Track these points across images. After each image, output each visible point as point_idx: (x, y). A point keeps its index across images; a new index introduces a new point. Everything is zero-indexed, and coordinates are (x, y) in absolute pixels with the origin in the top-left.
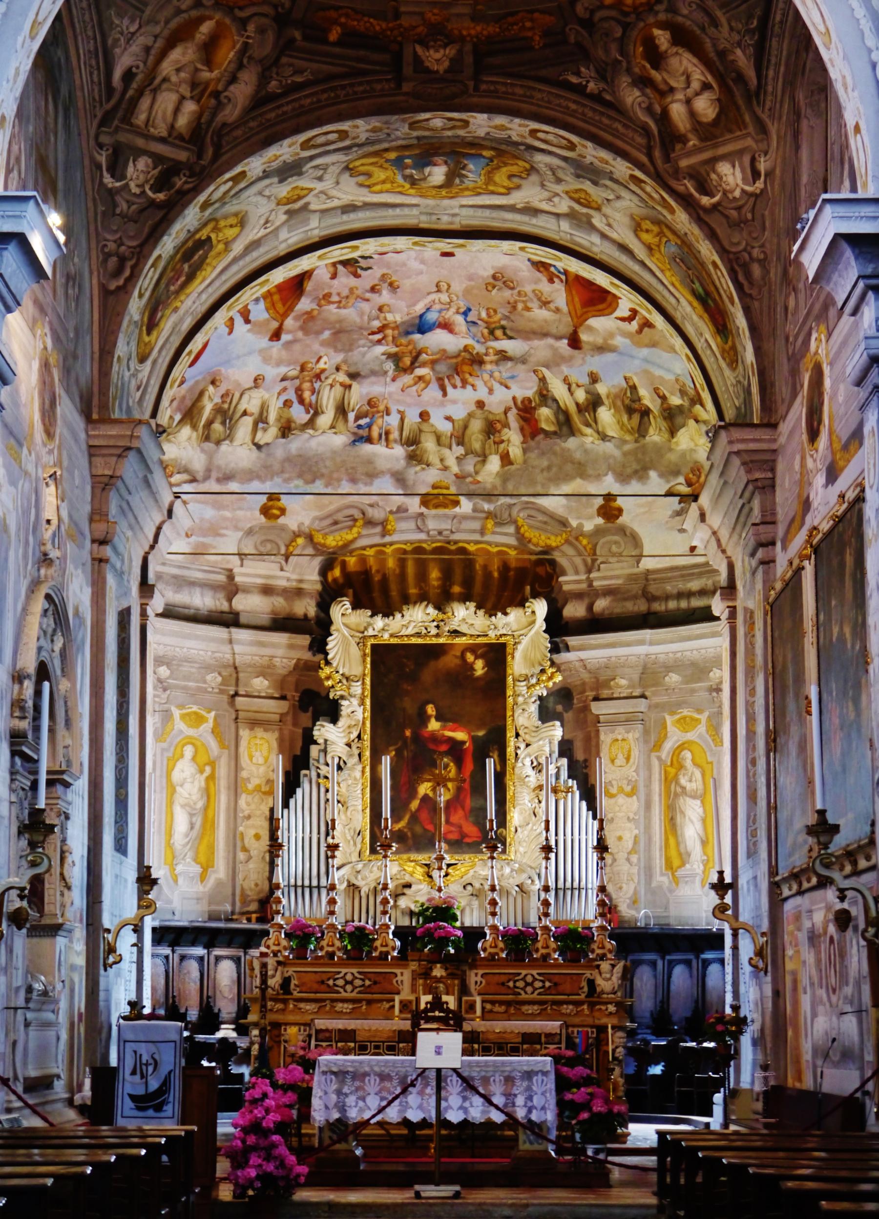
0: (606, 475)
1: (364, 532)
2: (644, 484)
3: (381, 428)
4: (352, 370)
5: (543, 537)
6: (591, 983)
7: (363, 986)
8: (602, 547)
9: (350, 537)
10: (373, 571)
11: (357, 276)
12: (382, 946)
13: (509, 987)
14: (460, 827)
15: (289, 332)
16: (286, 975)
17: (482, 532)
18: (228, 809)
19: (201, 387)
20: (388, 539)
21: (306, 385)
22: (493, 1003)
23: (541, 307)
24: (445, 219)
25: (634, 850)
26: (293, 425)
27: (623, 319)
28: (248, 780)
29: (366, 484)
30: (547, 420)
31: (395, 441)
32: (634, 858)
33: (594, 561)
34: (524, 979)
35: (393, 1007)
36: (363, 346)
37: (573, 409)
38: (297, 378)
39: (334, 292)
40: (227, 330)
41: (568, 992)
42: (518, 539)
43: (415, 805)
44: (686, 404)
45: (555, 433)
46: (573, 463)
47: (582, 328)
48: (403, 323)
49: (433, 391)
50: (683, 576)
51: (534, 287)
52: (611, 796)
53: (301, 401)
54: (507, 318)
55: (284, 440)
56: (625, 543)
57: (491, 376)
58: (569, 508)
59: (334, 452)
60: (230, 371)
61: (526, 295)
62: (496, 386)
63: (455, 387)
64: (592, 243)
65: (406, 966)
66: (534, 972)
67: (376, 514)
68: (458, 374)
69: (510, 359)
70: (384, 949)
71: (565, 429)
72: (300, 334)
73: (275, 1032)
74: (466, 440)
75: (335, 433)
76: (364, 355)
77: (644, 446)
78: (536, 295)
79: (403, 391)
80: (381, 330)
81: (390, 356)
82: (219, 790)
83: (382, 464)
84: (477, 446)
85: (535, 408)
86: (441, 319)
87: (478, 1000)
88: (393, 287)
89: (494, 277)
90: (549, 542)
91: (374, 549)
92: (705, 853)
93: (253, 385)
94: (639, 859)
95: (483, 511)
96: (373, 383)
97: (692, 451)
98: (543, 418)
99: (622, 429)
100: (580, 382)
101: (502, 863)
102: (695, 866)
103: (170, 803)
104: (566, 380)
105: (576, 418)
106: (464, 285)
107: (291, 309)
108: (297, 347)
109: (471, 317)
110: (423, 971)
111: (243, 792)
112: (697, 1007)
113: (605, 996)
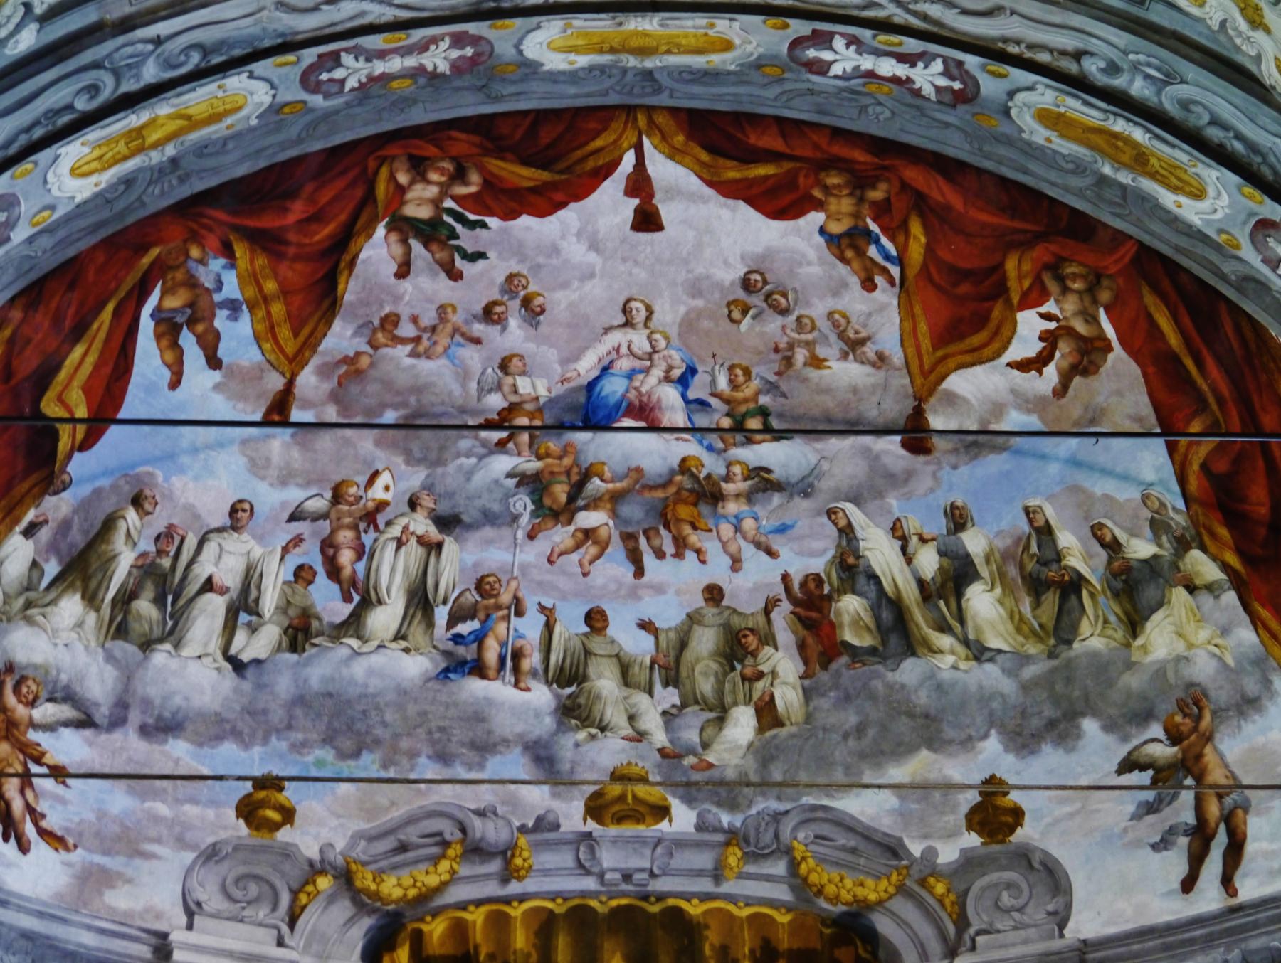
0: (985, 736)
1: (464, 871)
2: (1070, 750)
3: (503, 644)
4: (444, 508)
5: (848, 883)
8: (978, 899)
9: (433, 881)
10: (482, 958)
11: (455, 275)
15: (307, 405)
17: (717, 875)
19: (108, 507)
20: (514, 888)
21: (345, 536)
23: (844, 356)
27: (1023, 366)
29: (470, 767)
30: (857, 622)
31: (534, 674)
33: (962, 922)
37: (910, 594)
38: (325, 516)
39: (405, 312)
40: (167, 374)
42: (793, 888)
44: (1166, 552)
45: (873, 651)
46: (911, 715)
47: (933, 400)
48: (551, 401)
49: (614, 568)
50: (1167, 948)
51: (830, 304)
53: (334, 572)
54: (771, 387)
55: (294, 657)
56: (1031, 887)
57: (738, 529)
58: (901, 814)
59: (403, 692)
60: (177, 482)
61: (813, 328)
62: (748, 552)
63: (660, 555)
67: (490, 832)
69: (777, 486)
71: (894, 640)
74: (684, 672)
76: (469, 475)
77: (1069, 664)
78: (836, 325)
79: (550, 561)
83: (505, 725)
84: (706, 686)
85: (829, 598)
86: (632, 395)
88: (532, 310)
89: (746, 284)
90: (860, 892)
91: (484, 909)
93: (226, 521)
95: (718, 829)
96: (489, 542)
97: (1179, 659)
98: (846, 619)
99: (1018, 630)
104: (897, 531)
105: (919, 617)
106: (682, 310)
107: (309, 345)
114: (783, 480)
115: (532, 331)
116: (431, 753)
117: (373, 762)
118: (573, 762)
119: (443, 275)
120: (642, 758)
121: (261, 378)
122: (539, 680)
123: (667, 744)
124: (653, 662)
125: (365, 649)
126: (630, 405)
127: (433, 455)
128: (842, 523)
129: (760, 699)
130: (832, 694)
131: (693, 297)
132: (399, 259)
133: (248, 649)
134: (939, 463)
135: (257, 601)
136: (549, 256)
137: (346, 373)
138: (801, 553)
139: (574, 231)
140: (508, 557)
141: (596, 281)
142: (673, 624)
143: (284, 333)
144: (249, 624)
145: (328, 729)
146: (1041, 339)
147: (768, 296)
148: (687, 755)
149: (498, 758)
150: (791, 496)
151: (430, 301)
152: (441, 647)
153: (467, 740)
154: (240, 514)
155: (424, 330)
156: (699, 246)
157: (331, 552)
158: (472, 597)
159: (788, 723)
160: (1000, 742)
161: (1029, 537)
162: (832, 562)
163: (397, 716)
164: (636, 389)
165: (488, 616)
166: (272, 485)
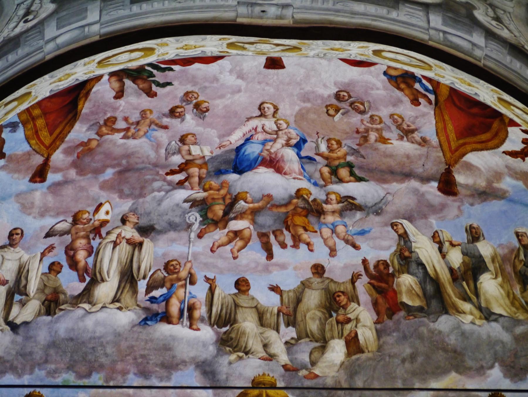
0: (492, 367)
3: (182, 302)
4: (144, 222)
11: (151, 94)
15: (57, 170)
21: (81, 243)
23: (401, 138)
24: (272, 11)
26: (62, 297)
27: (513, 154)
29: (161, 379)
30: (410, 291)
31: (202, 320)
36: (159, 191)
37: (445, 276)
38: (68, 232)
39: (119, 115)
45: (420, 309)
46: (445, 350)
47: (457, 166)
51: (391, 110)
53: (73, 264)
54: (354, 152)
55: (49, 318)
57: (333, 231)
59: (118, 335)
61: (381, 122)
62: (340, 245)
63: (283, 246)
64: (474, 45)
68: (288, 229)
69: (359, 208)
71: (434, 303)
72: (72, 173)
74: (299, 317)
75: (120, 309)
76: (160, 202)
78: (395, 121)
79: (212, 251)
80: (183, 168)
81: (194, 203)
84: (314, 326)
85: (393, 275)
86: (265, 154)
89: (338, 96)
93: (7, 242)
96: (173, 241)
98: (404, 289)
99: (513, 304)
100: (455, 241)
104: (435, 238)
105: (449, 289)
106: (297, 108)
107: (61, 138)
108: (68, 191)
109: (307, 150)
114: (363, 204)
115: (201, 121)
116: (136, 372)
117: (100, 379)
118: (227, 374)
119: (144, 95)
120: (273, 371)
121: (29, 159)
122: (205, 324)
123: (289, 362)
124: (279, 311)
125: (93, 310)
126: (264, 159)
127: (137, 192)
128: (401, 231)
129: (349, 335)
130: (395, 334)
131: (304, 102)
132: (117, 89)
133: (20, 316)
134: (462, 201)
135: (25, 286)
136: (212, 82)
137: (82, 151)
138: (375, 248)
139: (228, 70)
140: (185, 249)
141: (242, 94)
142: (292, 287)
143: (44, 134)
144: (20, 301)
145: (70, 360)
146: (523, 142)
147: (352, 104)
148: (302, 369)
149: (179, 373)
150: (368, 214)
151: (136, 109)
152: (142, 305)
153: (159, 362)
154: (15, 236)
155: (132, 124)
156: (307, 77)
157: (72, 253)
158: (162, 274)
159: (366, 351)
160: (501, 371)
161: (519, 250)
162: (394, 254)
163: (114, 350)
164: (267, 150)
165: (172, 285)
166: (35, 218)
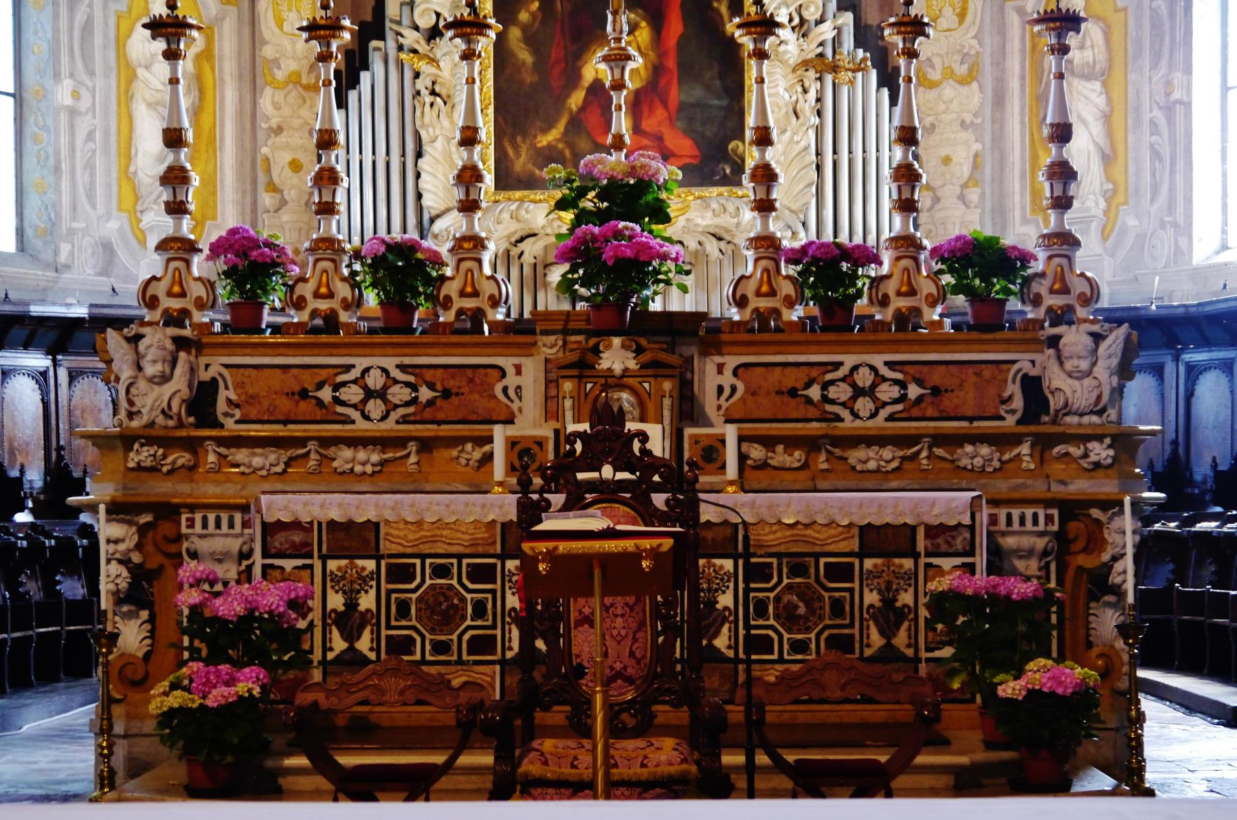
6: (1033, 387)
7: (414, 401)
12: (463, 294)
13: (809, 401)
14: (659, 138)
16: (205, 376)
18: (240, 114)
22: (769, 442)
25: (973, 180)
28: (276, 62)
32: (973, 195)
34: (848, 379)
35: (489, 457)
41: (970, 413)
43: (576, 99)
52: (933, 85)
65: (527, 349)
66: (878, 360)
70: (469, 303)
73: (166, 528)
82: (222, 80)
87: (731, 433)
92: (1109, 178)
94: (982, 196)
101: (738, 202)
102: (1090, 203)
103: (126, 96)
110: (573, 357)
111: (267, 84)
112: (1175, 452)
113: (1068, 419)
